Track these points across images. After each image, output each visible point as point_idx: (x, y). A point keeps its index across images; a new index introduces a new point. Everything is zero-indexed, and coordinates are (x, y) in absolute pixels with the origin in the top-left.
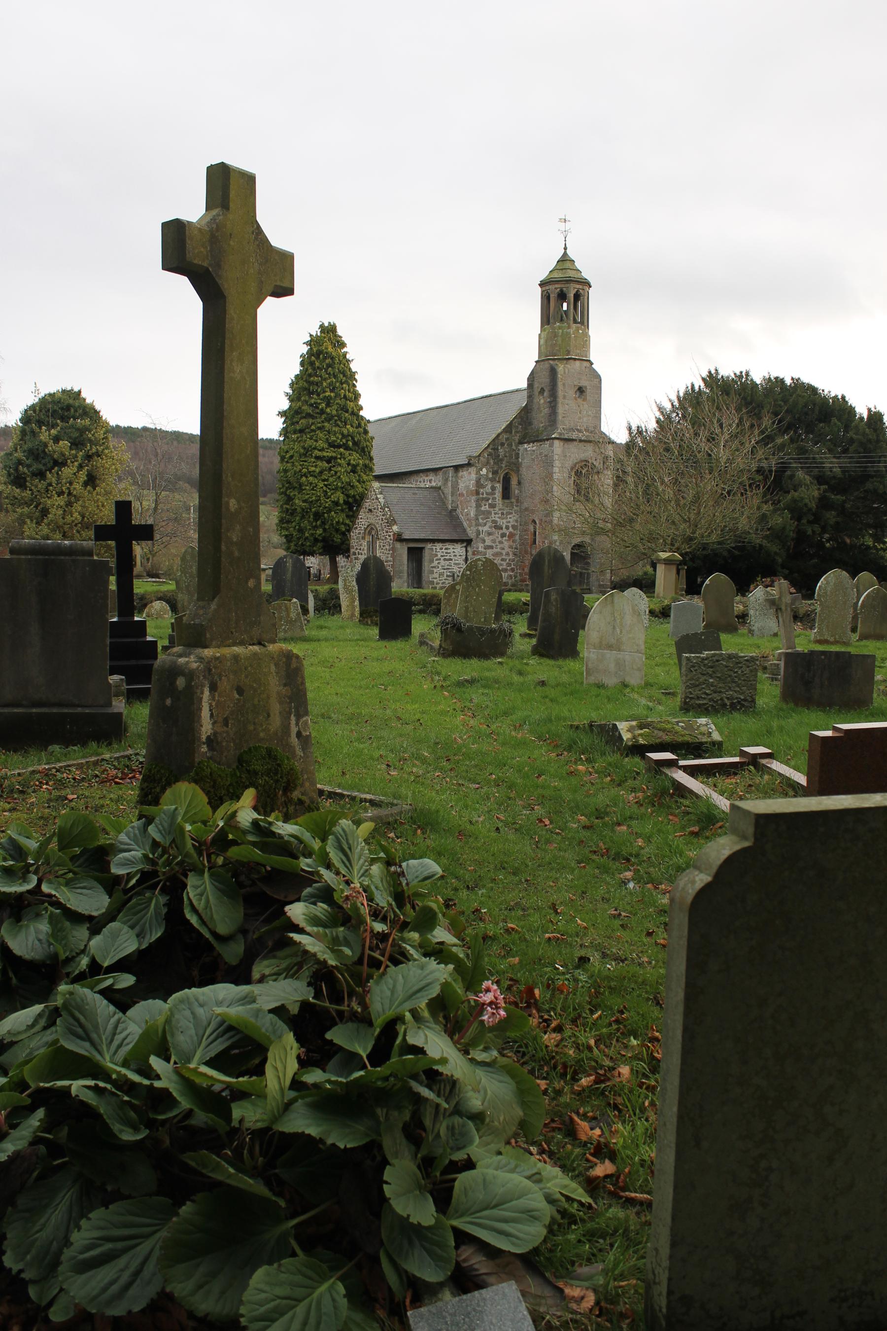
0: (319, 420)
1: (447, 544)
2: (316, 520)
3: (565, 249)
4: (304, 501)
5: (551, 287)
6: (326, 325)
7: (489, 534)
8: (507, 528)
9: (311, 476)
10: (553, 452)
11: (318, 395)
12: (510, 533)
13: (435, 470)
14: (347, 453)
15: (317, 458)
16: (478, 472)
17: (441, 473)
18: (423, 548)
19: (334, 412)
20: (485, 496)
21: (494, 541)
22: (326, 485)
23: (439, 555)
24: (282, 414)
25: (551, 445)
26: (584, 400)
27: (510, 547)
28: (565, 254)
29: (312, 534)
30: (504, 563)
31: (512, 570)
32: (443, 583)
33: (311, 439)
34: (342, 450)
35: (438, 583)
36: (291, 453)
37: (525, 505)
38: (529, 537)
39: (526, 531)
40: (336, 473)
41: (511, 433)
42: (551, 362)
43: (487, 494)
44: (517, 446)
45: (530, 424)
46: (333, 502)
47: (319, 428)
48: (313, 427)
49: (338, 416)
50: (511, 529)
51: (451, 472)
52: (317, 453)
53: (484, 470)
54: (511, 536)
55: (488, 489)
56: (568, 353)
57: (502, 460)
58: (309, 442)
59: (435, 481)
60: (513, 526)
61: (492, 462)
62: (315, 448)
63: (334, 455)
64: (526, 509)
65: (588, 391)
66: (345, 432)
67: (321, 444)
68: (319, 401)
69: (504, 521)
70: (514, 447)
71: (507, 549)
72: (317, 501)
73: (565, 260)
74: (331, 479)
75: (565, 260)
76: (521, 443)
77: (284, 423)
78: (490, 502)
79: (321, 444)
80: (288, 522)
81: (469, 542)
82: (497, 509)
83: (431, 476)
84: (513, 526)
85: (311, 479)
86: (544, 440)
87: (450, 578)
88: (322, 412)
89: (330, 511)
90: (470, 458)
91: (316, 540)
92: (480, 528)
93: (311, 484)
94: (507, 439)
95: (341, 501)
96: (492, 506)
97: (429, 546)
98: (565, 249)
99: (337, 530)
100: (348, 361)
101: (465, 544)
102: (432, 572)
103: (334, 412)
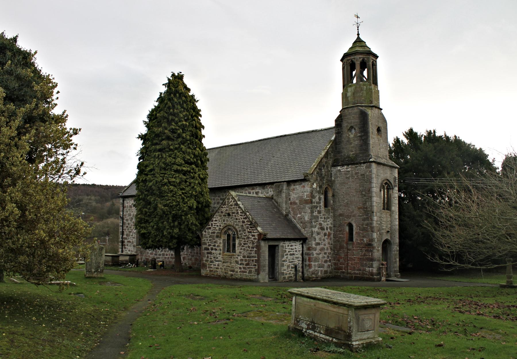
0: (176, 142)
1: (291, 242)
2: (174, 221)
3: (358, 34)
4: (165, 206)
5: (356, 57)
6: (176, 74)
7: (318, 234)
8: (327, 229)
9: (171, 185)
10: (371, 172)
11: (177, 123)
12: (329, 232)
14: (197, 169)
15: (177, 171)
16: (311, 187)
18: (278, 245)
19: (188, 137)
20: (315, 204)
21: (320, 239)
22: (183, 193)
23: (287, 250)
24: (141, 137)
25: (370, 167)
26: (381, 136)
27: (329, 244)
28: (358, 38)
29: (170, 233)
30: (326, 256)
31: (330, 261)
32: (290, 273)
33: (170, 156)
34: (194, 166)
35: (286, 274)
36: (151, 167)
37: (340, 211)
38: (346, 236)
39: (340, 231)
40: (190, 183)
41: (328, 158)
42: (361, 108)
43: (317, 203)
44: (331, 168)
45: (339, 152)
46: (189, 207)
47: (176, 149)
48: (171, 147)
49: (190, 140)
50: (329, 230)
51: (285, 186)
52: (175, 167)
53: (315, 186)
54: (329, 234)
55: (317, 199)
56: (371, 103)
57: (324, 178)
58: (169, 160)
59: (270, 192)
60: (330, 228)
61: (319, 178)
62: (174, 164)
63: (189, 169)
64: (341, 215)
65: (383, 130)
66: (196, 153)
67: (179, 160)
68: (177, 128)
69: (326, 223)
70: (329, 169)
71: (327, 245)
72: (177, 206)
73: (359, 41)
74: (187, 189)
75: (359, 41)
76: (334, 165)
77: (142, 144)
78: (318, 209)
79: (179, 160)
80: (147, 222)
82: (322, 214)
83: (258, 189)
84: (330, 228)
85: (172, 187)
86: (361, 163)
87: (293, 269)
88: (179, 136)
89: (186, 215)
90: (306, 175)
91: (172, 237)
92: (313, 229)
93: (172, 191)
94: (326, 162)
95: (195, 207)
96: (319, 212)
97: (281, 244)
98: (358, 34)
99: (189, 229)
100: (195, 100)
101: (301, 242)
103: (188, 137)
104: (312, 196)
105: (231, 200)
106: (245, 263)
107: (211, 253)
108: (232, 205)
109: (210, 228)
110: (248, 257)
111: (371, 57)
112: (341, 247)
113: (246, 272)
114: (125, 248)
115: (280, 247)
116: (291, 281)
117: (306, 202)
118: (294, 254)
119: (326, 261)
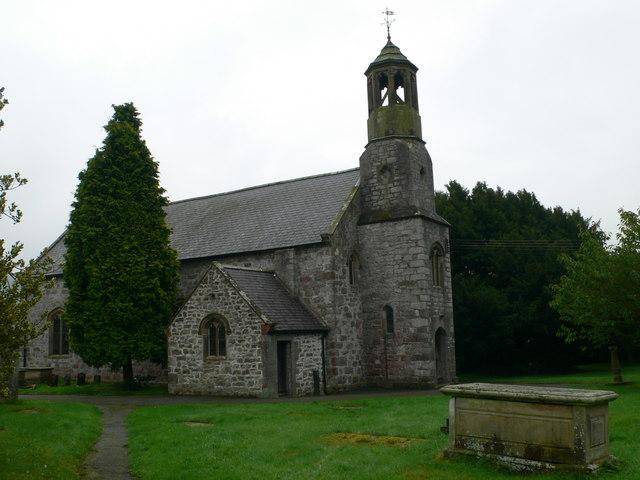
3: (389, 38)
13: (258, 254)
17: (277, 257)
18: (289, 342)
28: (389, 43)
51: (292, 254)
53: (337, 253)
59: (265, 264)
75: (390, 48)
81: (324, 333)
84: (359, 314)
96: (344, 291)
97: (295, 339)
98: (389, 38)
102: (298, 372)
104: (334, 266)
105: (215, 275)
106: (242, 370)
107: (183, 358)
108: (217, 283)
109: (182, 320)
110: (247, 361)
111: (409, 70)
112: (376, 342)
113: (243, 384)
114: (29, 359)
115: (293, 345)
116: (308, 395)
117: (325, 276)
118: (311, 355)
119: (355, 364)
